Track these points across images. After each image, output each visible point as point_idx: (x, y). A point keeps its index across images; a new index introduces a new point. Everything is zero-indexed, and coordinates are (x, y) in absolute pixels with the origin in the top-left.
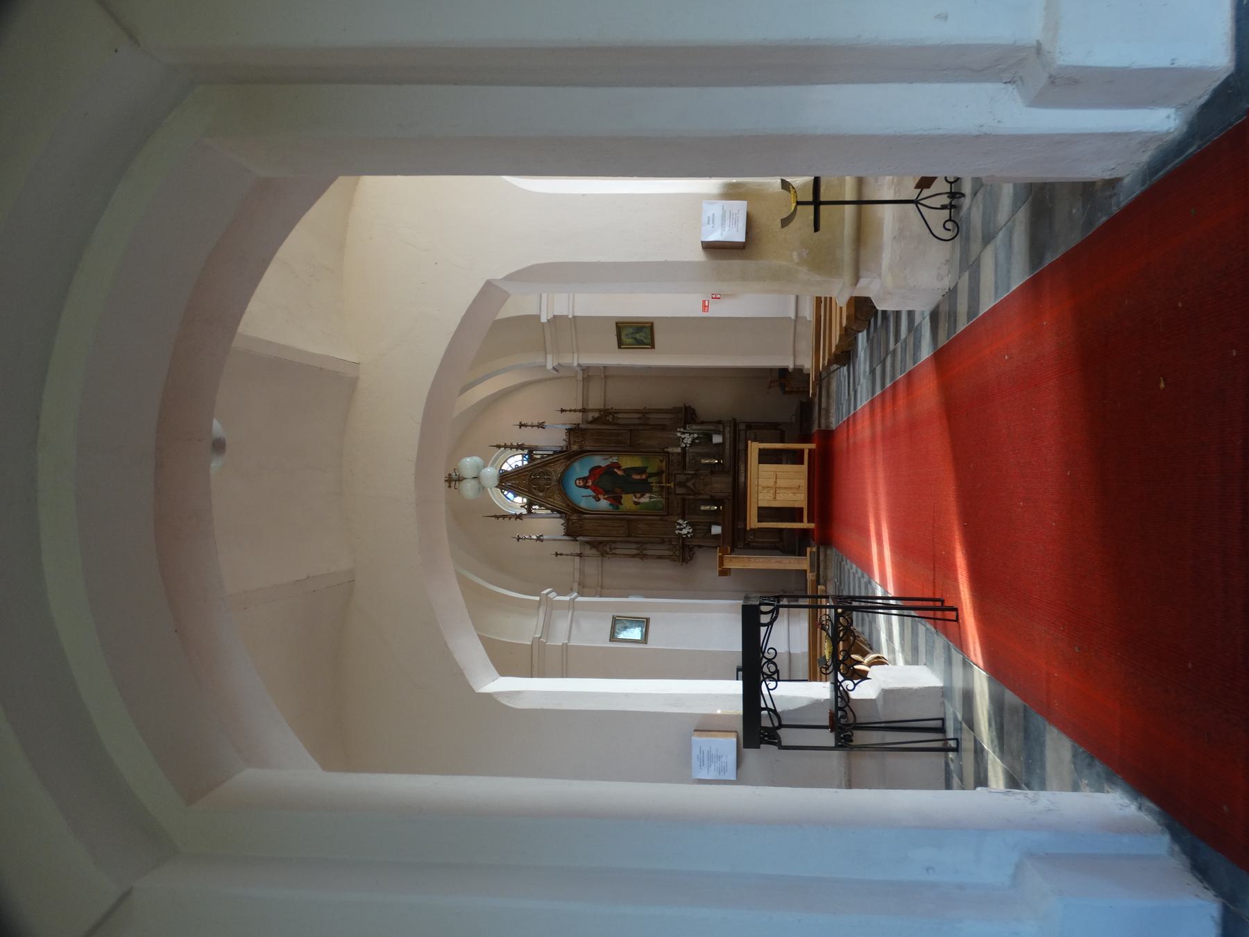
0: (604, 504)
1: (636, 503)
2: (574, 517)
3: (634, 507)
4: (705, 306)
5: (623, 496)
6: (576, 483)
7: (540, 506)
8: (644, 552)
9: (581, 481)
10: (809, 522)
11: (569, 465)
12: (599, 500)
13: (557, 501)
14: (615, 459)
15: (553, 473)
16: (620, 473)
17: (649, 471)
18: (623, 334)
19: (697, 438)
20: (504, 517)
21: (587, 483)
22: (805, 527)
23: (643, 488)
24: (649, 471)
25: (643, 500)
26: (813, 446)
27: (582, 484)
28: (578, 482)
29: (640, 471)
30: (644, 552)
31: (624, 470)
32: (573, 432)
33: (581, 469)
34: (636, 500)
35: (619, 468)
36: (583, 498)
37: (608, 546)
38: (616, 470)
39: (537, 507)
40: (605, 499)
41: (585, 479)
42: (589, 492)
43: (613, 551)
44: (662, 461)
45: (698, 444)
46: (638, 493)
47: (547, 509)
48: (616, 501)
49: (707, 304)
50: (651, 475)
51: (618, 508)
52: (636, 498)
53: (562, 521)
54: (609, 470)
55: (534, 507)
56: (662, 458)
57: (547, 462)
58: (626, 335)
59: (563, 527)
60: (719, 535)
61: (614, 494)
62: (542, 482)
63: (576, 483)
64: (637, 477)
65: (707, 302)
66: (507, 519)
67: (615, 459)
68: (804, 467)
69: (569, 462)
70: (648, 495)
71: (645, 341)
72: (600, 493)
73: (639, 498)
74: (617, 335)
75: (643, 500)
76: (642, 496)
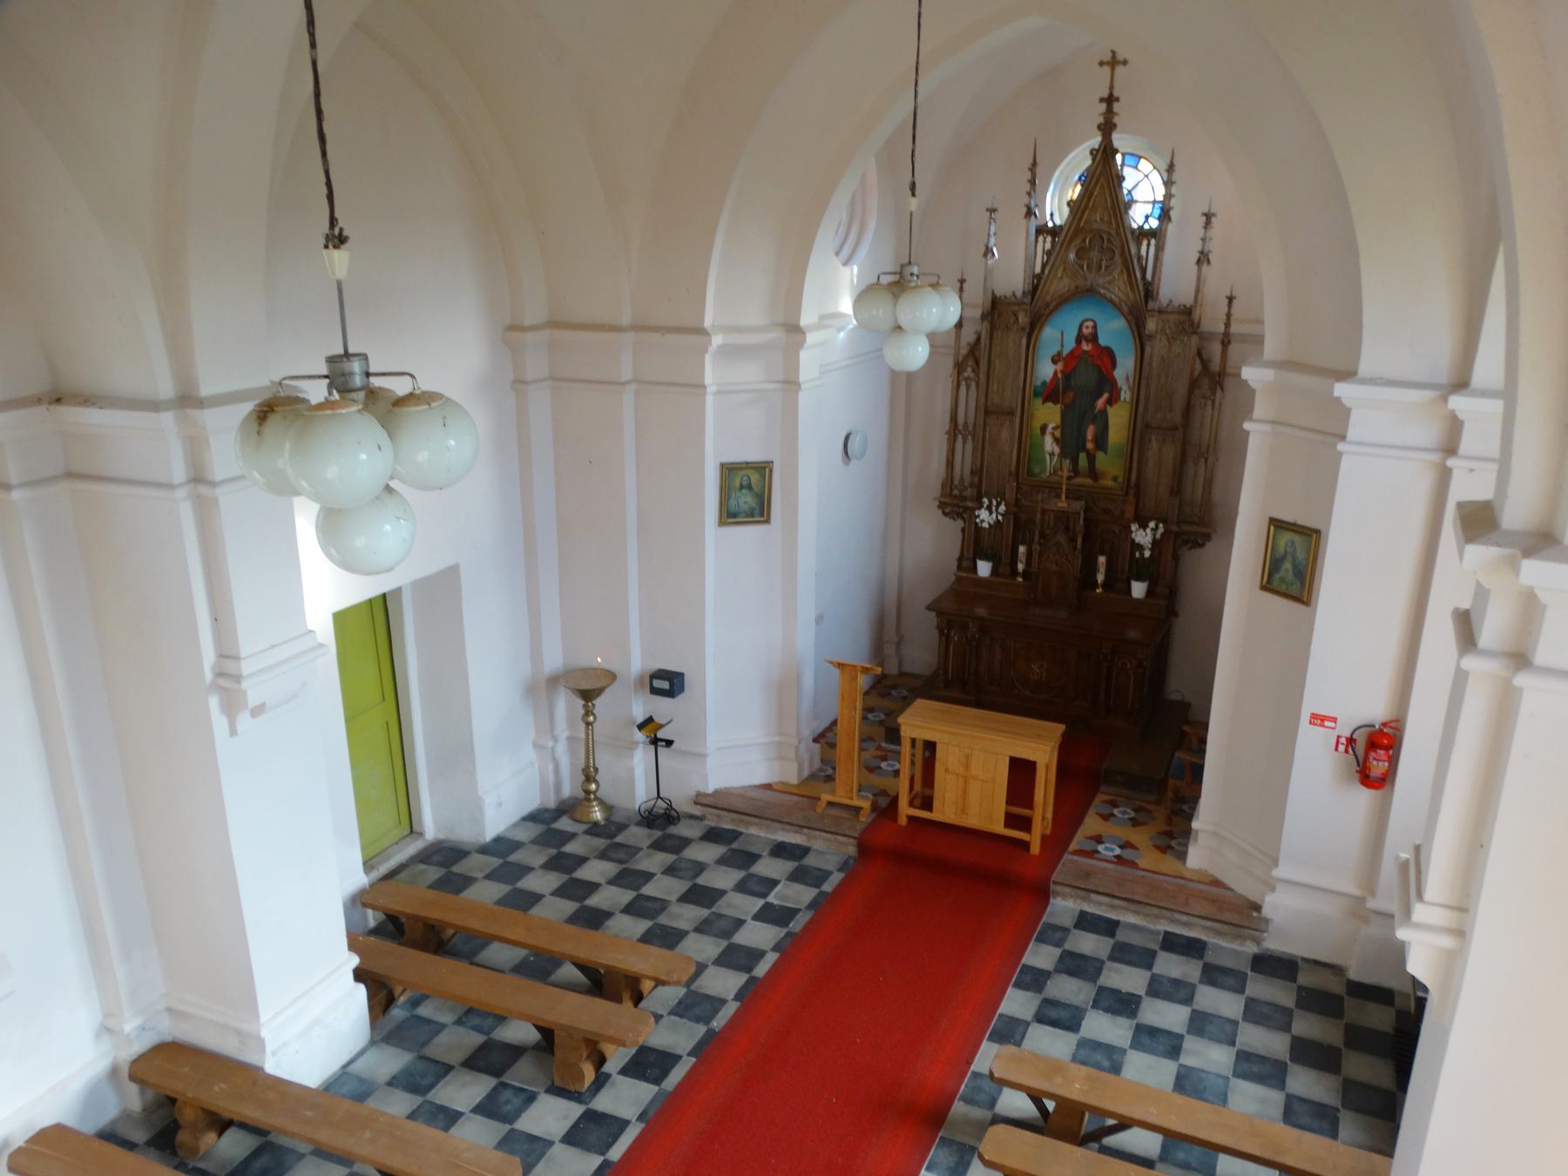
0: (1046, 370)
1: (1043, 429)
2: (1023, 319)
3: (1037, 424)
4: (1322, 721)
5: (1059, 406)
6: (1087, 320)
7: (1049, 253)
8: (960, 436)
9: (1090, 330)
10: (911, 818)
11: (1120, 310)
12: (1054, 361)
13: (1059, 285)
14: (1125, 395)
15: (1108, 278)
16: (1100, 403)
17: (1100, 455)
18: (1297, 539)
19: (1116, 584)
20: (1032, 182)
21: (1087, 341)
22: (900, 810)
23: (1071, 443)
24: (1100, 455)
25: (1048, 440)
26: (1035, 849)
27: (1085, 331)
28: (1090, 324)
29: (1101, 442)
30: (960, 436)
31: (1104, 412)
32: (1186, 318)
33: (1113, 331)
34: (1049, 429)
35: (1110, 402)
36: (1058, 335)
37: (972, 375)
38: (1106, 396)
39: (1048, 246)
40: (1055, 373)
41: (1094, 338)
42: (1070, 345)
43: (963, 383)
44: (1115, 479)
45: (1132, 554)
46: (1062, 433)
47: (1044, 266)
48: (1051, 393)
49: (1327, 723)
50: (1091, 459)
51: (1036, 394)
52: (1054, 428)
53: (1019, 294)
54: (1106, 383)
55: (1049, 239)
56: (1120, 480)
57: (1129, 265)
58: (1293, 544)
59: (1009, 294)
60: (976, 573)
61: (1064, 392)
62: (1095, 255)
63: (1087, 320)
64: (1090, 432)
65: (1332, 725)
66: (1027, 187)
67: (1125, 395)
68: (999, 827)
69: (1125, 309)
70: (1057, 450)
71: (1278, 576)
72: (1066, 366)
73: (1053, 434)
74: (1294, 524)
75: (1048, 440)
76: (1056, 440)
